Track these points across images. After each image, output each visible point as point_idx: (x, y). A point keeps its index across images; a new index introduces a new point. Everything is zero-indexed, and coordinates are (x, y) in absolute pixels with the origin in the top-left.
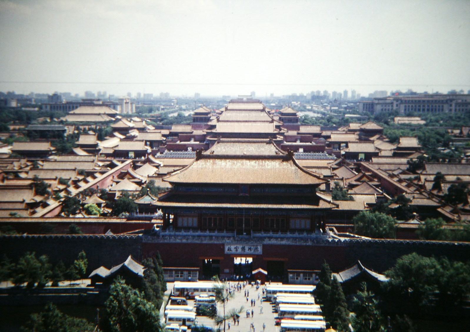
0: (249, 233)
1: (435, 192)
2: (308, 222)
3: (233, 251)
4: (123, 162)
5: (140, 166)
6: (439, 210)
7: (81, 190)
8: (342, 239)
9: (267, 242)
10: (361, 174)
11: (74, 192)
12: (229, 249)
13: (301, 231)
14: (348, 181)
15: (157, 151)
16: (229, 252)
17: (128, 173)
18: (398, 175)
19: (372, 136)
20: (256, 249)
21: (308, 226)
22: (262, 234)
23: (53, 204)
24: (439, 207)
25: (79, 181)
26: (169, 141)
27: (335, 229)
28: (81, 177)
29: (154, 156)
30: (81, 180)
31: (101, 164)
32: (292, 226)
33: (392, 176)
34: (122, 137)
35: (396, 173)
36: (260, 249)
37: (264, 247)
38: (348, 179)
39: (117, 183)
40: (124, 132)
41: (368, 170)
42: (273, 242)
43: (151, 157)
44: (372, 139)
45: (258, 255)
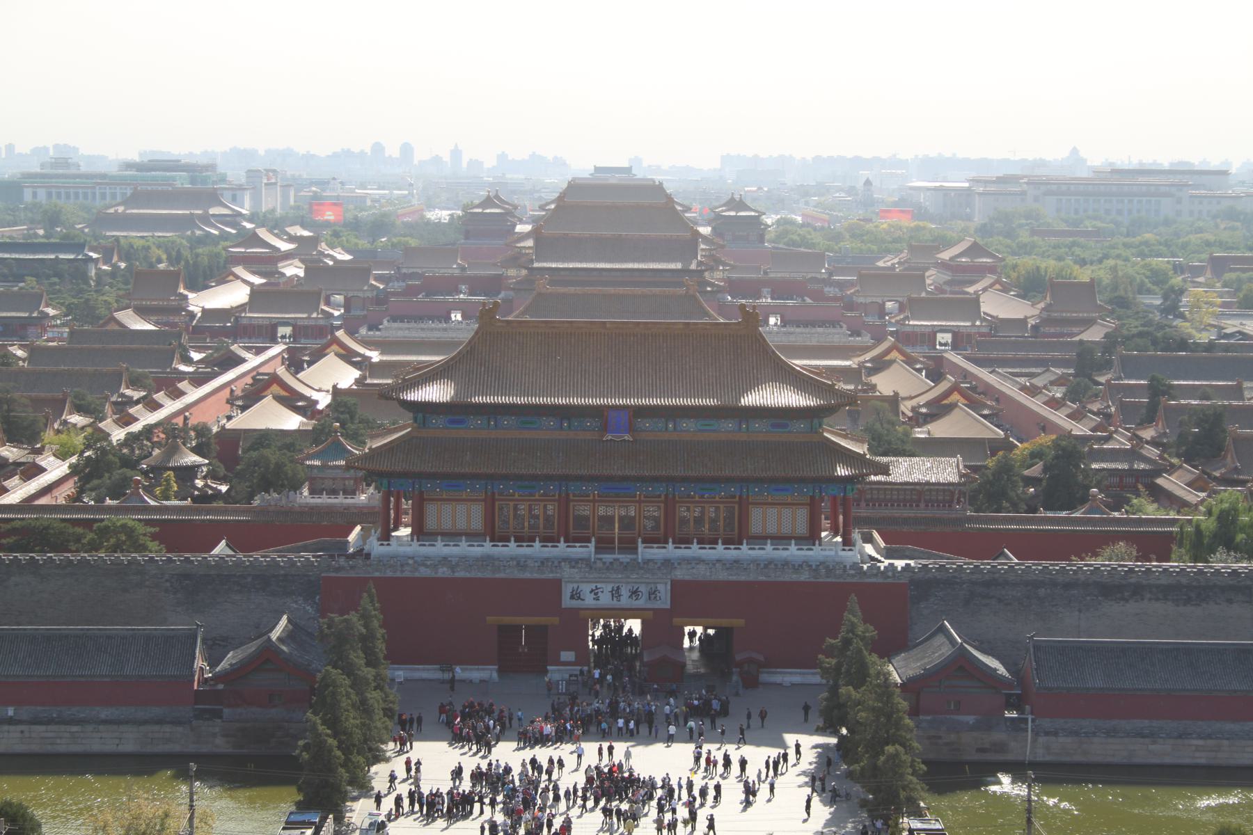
0: (629, 546)
1: (1148, 434)
2: (802, 514)
3: (589, 601)
4: (259, 351)
5: (310, 364)
6: (1159, 481)
7: (136, 427)
8: (900, 564)
9: (680, 574)
10: (943, 386)
11: (118, 435)
12: (576, 595)
13: (780, 539)
14: (909, 404)
15: (362, 321)
16: (575, 604)
17: (275, 379)
18: (1045, 387)
19: (972, 283)
20: (652, 594)
21: (802, 528)
22: (670, 551)
23: (55, 469)
24: (1158, 473)
25: (132, 402)
26: (395, 294)
27: (876, 535)
28: (136, 395)
29: (351, 333)
30: (138, 402)
31: (196, 356)
32: (755, 528)
33: (1032, 391)
34: (258, 280)
35: (1039, 382)
36: (664, 591)
37: (676, 586)
38: (911, 398)
39: (243, 408)
40: (263, 268)
41: (966, 375)
42: (702, 573)
43: (340, 334)
44: (971, 290)
45: (656, 611)
